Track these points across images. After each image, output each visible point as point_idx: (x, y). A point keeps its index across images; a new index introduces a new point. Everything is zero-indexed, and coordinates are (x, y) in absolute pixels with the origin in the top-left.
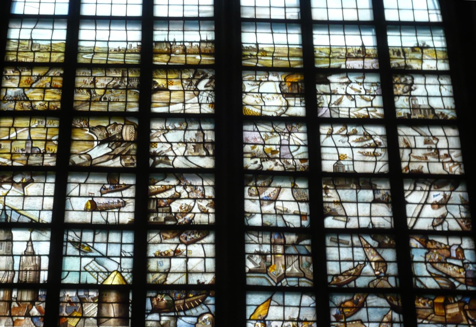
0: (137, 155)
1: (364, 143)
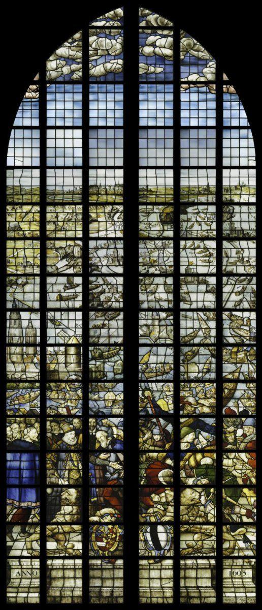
1: (203, 254)
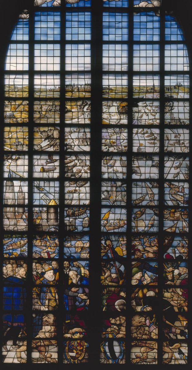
1: (150, 138)
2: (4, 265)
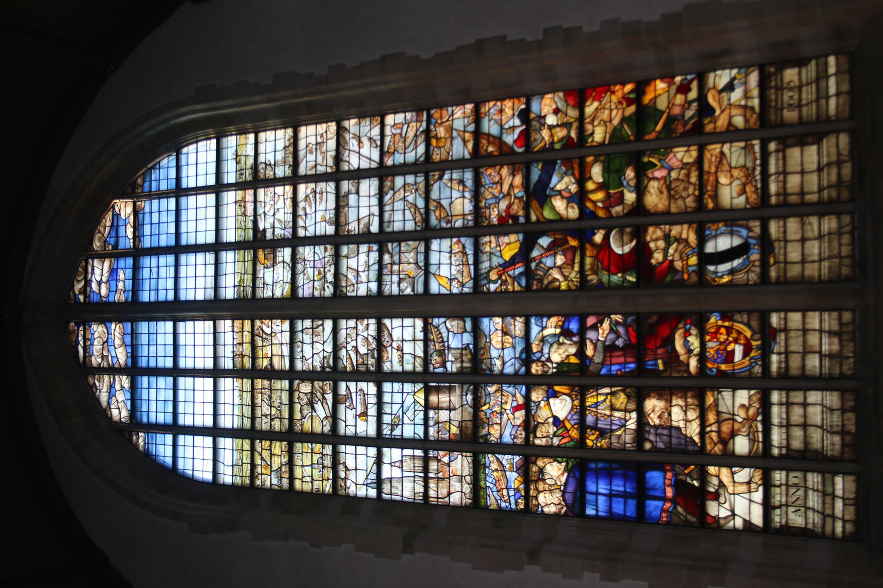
0: (323, 381)
2: (540, 509)
